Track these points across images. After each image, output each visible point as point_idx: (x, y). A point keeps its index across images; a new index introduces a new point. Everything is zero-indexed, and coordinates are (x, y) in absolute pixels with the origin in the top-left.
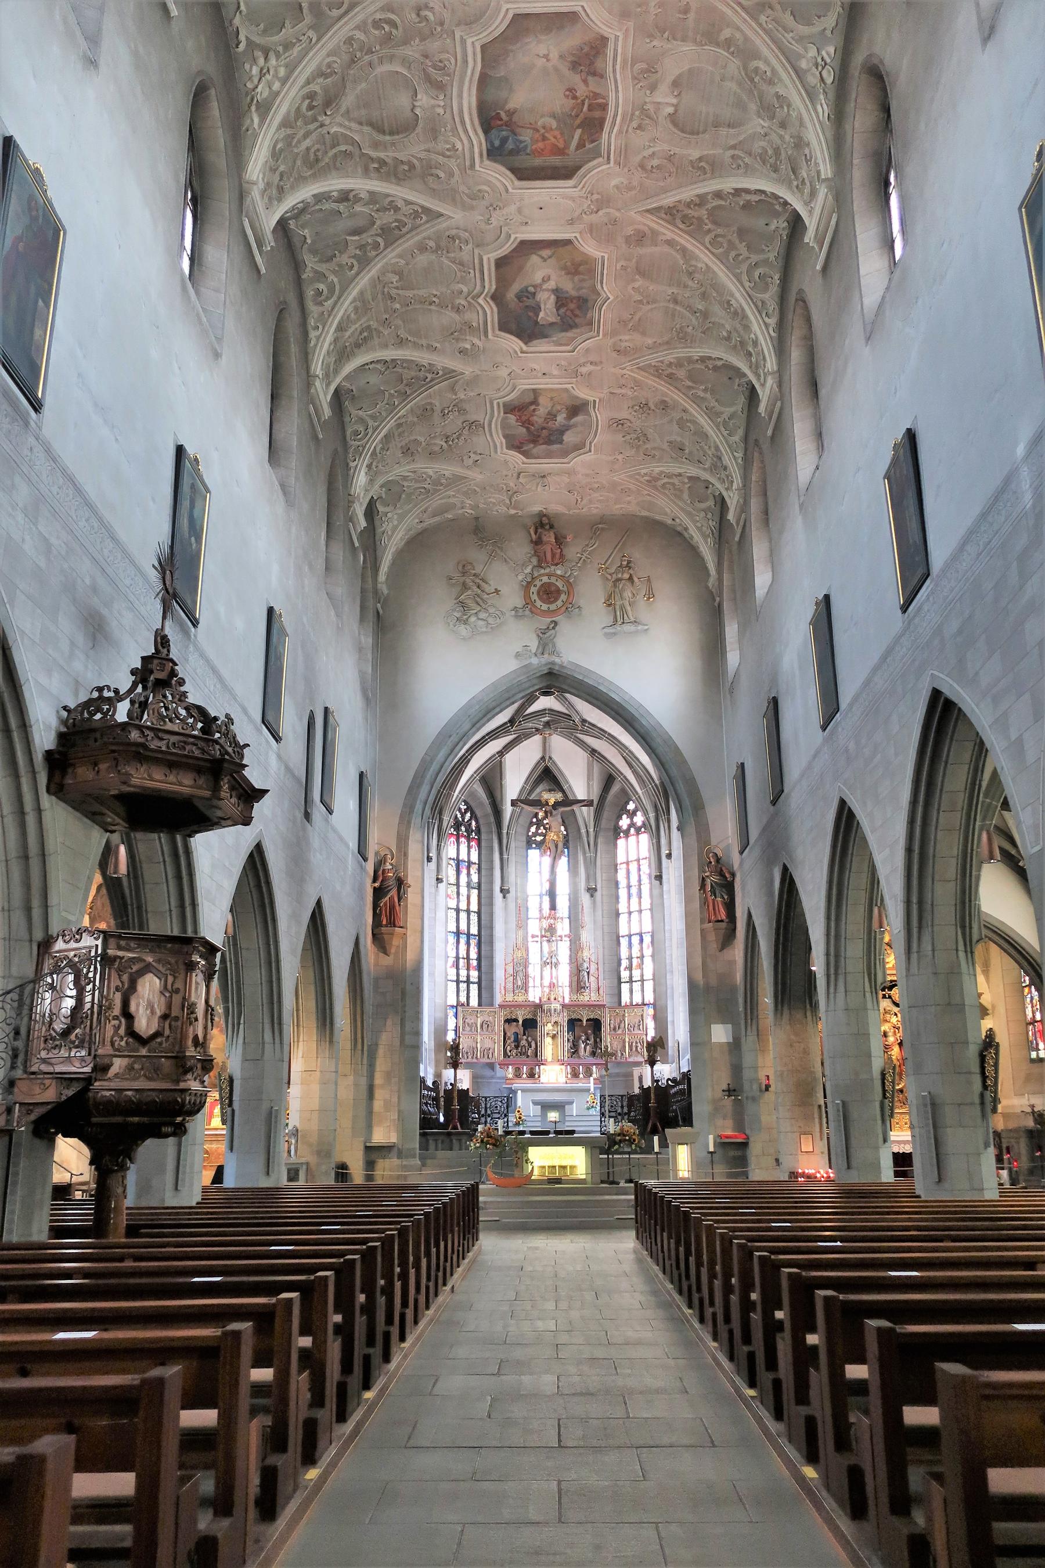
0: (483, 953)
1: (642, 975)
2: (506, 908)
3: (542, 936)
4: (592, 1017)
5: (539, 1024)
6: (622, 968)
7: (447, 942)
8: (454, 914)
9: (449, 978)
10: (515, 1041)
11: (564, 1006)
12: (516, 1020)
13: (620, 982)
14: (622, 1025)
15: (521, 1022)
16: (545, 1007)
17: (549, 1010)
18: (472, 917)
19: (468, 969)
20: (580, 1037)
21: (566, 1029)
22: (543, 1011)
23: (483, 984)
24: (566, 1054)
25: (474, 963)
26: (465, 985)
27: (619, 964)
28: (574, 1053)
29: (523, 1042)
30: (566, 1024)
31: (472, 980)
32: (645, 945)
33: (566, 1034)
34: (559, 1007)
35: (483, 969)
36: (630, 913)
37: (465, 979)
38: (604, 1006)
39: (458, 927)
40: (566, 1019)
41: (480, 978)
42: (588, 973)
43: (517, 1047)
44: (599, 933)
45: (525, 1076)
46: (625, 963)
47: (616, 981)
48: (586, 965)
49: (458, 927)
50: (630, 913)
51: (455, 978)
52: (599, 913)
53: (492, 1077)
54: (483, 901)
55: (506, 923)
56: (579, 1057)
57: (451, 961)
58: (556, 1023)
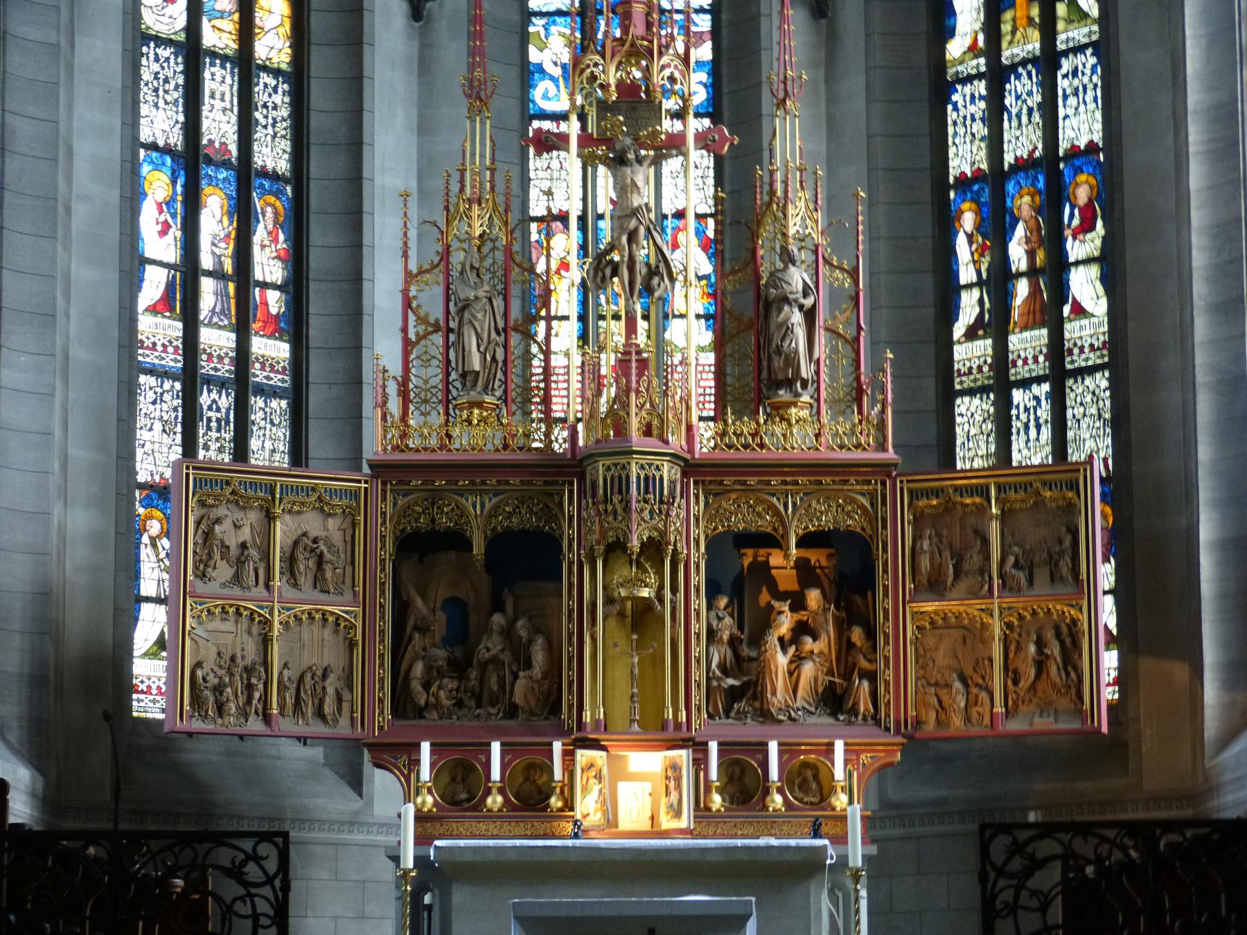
0: (317, 260)
1: (1057, 349)
2: (425, 66)
3: (585, 140)
4: (826, 521)
5: (571, 554)
6: (959, 330)
7: (133, 196)
8: (175, 69)
9: (147, 358)
10: (448, 641)
11: (691, 468)
12: (457, 541)
13: (947, 396)
14: (975, 559)
15: (478, 547)
16: (600, 471)
17: (621, 484)
18: (260, 95)
19: (242, 330)
20: (766, 620)
21: (699, 579)
22: (587, 490)
23: (316, 398)
24: (698, 697)
25: (275, 301)
26: (226, 401)
27: (949, 311)
28: (733, 695)
29: (491, 646)
30: (697, 555)
31: (259, 375)
32: (1071, 217)
33: (699, 603)
34: (669, 472)
35: (319, 327)
36: (998, 76)
37: (226, 369)
38: (884, 469)
39: (192, 127)
40: (699, 532)
41: (298, 365)
42: (810, 316)
43: (458, 667)
44: (855, 171)
45: (495, 801)
46: (969, 306)
47: (929, 386)
48: (797, 278)
49: (192, 127)
50: (998, 76)
51: (173, 361)
52: (855, 84)
53: (353, 823)
54: (317, 23)
55: (425, 128)
56: (765, 715)
57: (154, 284)
58: (654, 549)
